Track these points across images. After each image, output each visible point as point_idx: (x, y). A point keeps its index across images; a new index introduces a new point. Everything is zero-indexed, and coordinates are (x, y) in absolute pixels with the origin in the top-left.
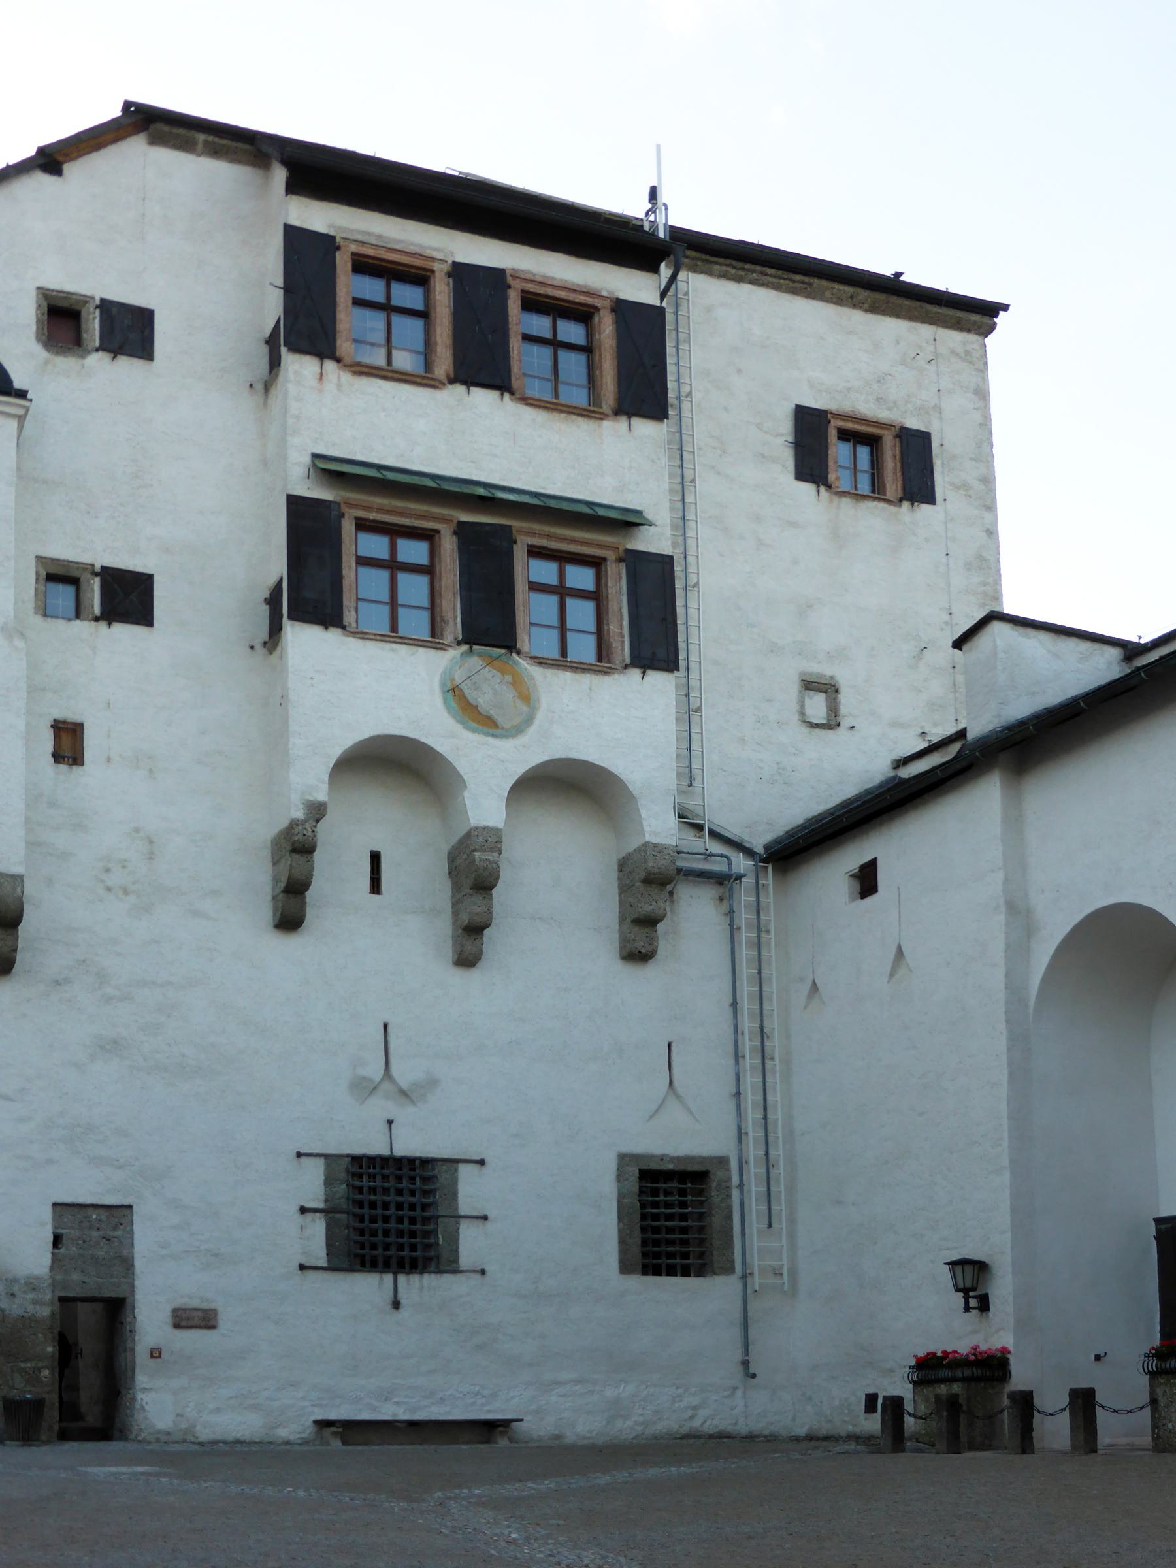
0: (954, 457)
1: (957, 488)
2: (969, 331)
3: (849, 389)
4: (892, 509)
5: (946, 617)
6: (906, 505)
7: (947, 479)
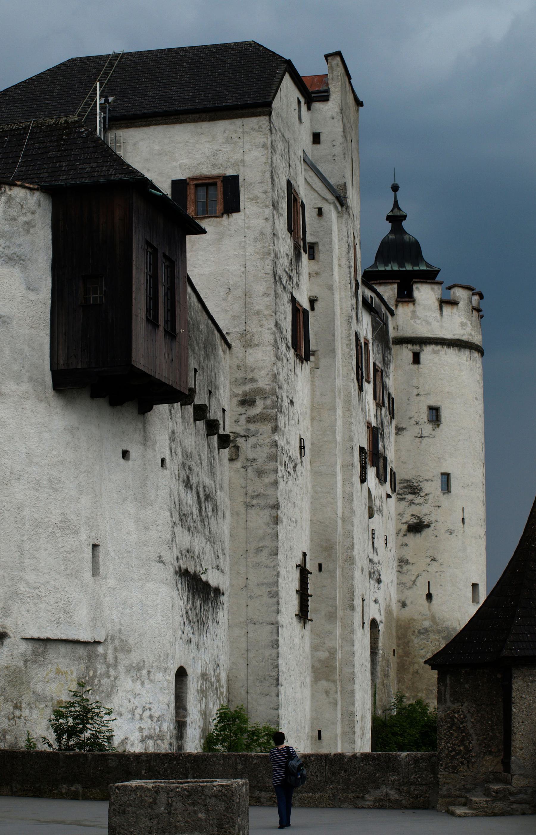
0: (251, 184)
1: (251, 200)
2: (260, 116)
3: (199, 164)
4: (218, 219)
5: (243, 269)
6: (225, 216)
7: (246, 196)
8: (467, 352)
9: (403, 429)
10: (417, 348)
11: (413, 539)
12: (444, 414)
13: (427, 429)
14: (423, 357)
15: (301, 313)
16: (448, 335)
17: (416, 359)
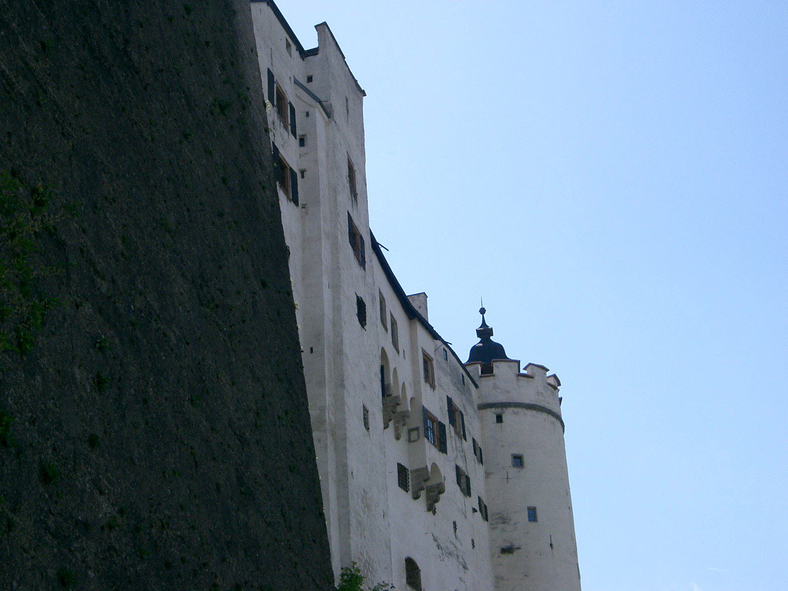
8: (545, 415)
9: (491, 473)
10: (499, 411)
11: (507, 558)
12: (526, 460)
13: (513, 471)
14: (504, 418)
15: (288, 169)
16: (527, 401)
17: (499, 419)
